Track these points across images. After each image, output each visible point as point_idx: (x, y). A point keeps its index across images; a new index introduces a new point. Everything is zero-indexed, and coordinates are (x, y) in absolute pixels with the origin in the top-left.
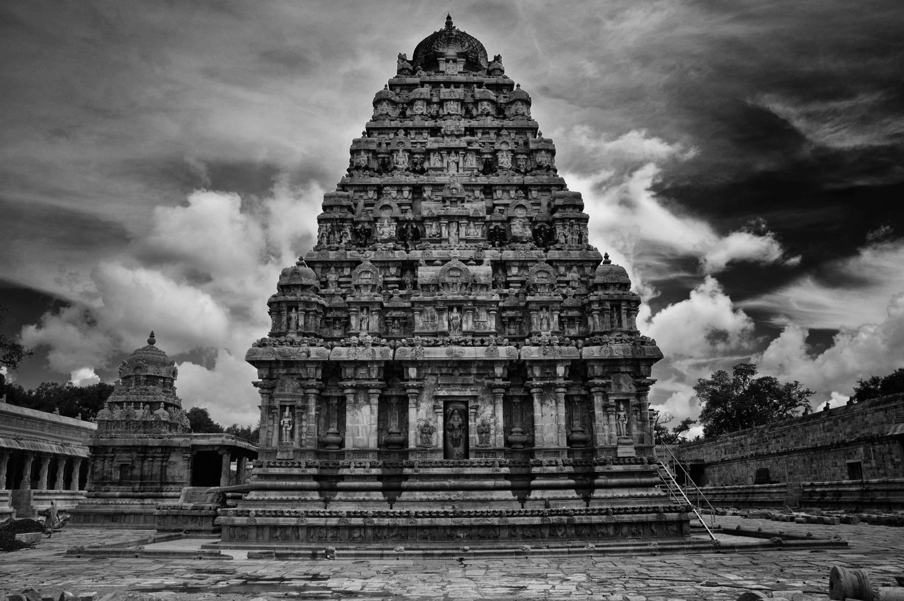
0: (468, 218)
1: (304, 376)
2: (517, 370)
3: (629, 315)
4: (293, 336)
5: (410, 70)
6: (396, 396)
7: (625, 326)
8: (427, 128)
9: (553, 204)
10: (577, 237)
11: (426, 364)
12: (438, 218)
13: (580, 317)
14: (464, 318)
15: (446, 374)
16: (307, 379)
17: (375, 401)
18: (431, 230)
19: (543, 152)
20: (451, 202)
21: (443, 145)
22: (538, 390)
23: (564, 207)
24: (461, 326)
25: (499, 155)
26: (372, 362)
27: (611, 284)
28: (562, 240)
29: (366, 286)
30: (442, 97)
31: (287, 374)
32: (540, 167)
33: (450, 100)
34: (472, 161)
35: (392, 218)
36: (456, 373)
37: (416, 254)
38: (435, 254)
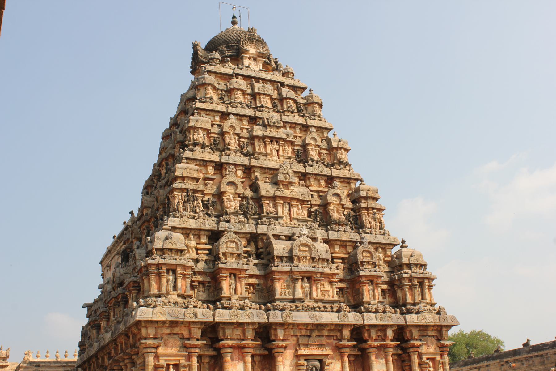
0: (297, 200)
1: (186, 336)
2: (358, 333)
3: (429, 290)
4: (174, 297)
5: (220, 61)
6: (260, 355)
7: (428, 300)
8: (246, 116)
9: (356, 196)
10: (378, 224)
11: (291, 327)
12: (274, 198)
13: (389, 290)
14: (314, 288)
15: (304, 335)
16: (188, 339)
17: (249, 359)
18: (268, 207)
19: (342, 150)
20: (283, 185)
21: (267, 134)
22: (375, 350)
23: (366, 198)
24: (310, 293)
25: (309, 148)
26: (248, 324)
27: (414, 264)
28: (368, 225)
29: (232, 254)
30: (256, 91)
31: (170, 334)
32: (340, 163)
33: (264, 94)
34: (289, 151)
35: (236, 194)
36: (314, 334)
37: (262, 229)
38: (279, 230)
